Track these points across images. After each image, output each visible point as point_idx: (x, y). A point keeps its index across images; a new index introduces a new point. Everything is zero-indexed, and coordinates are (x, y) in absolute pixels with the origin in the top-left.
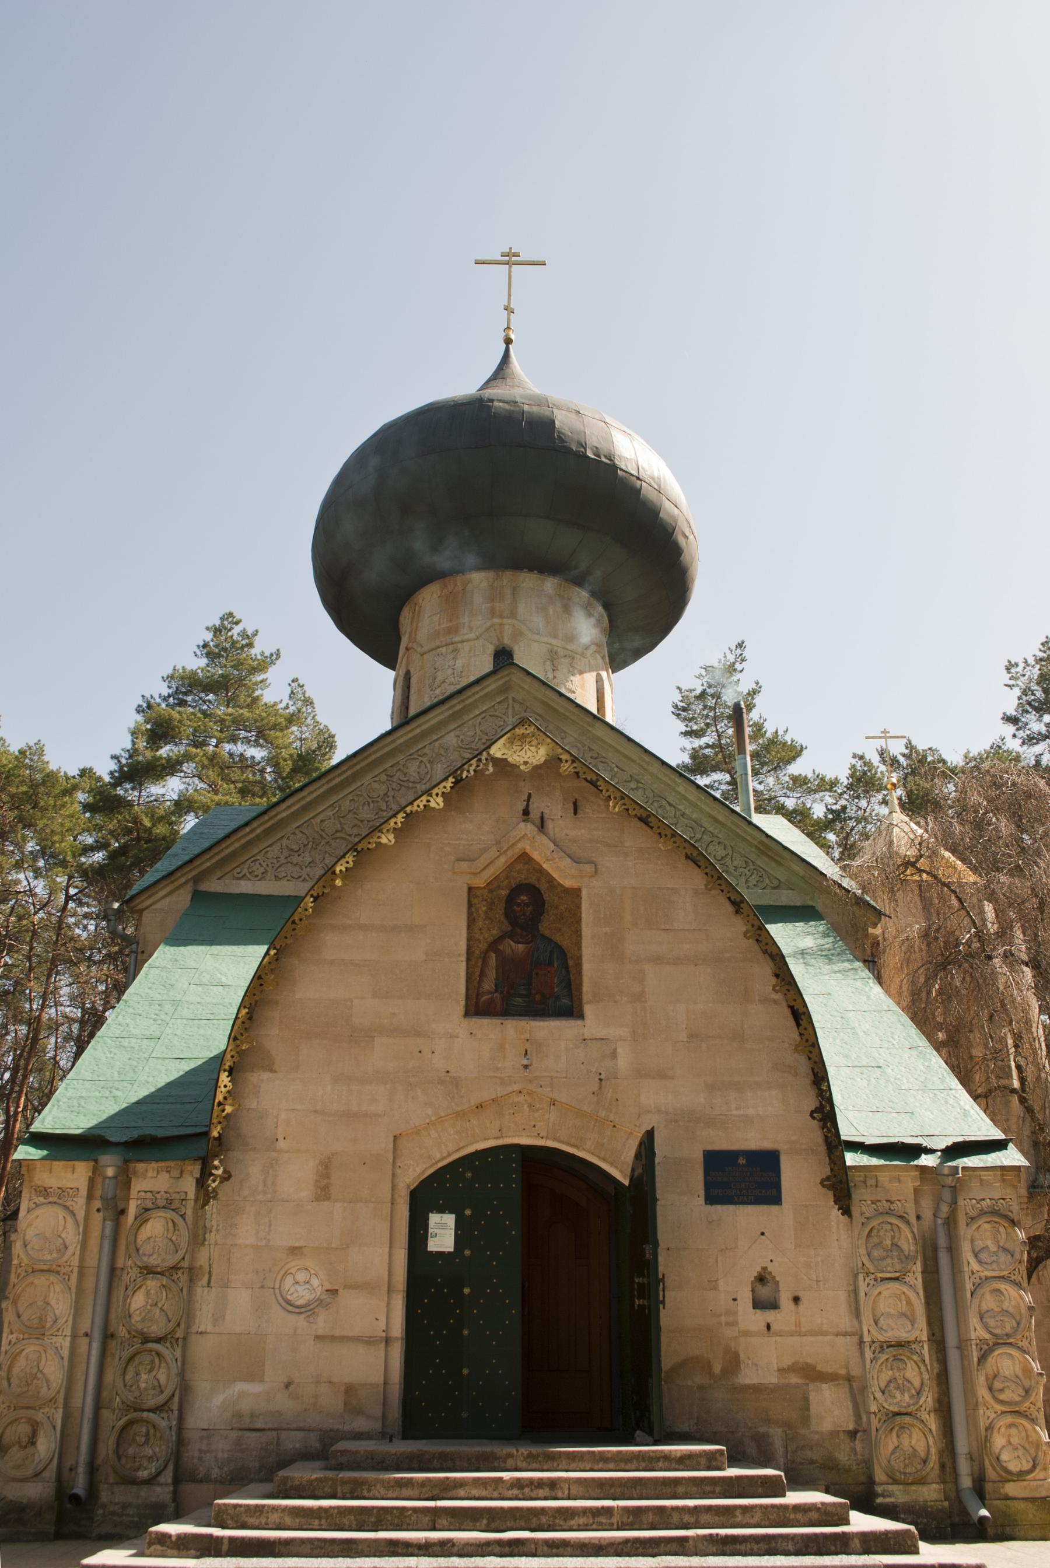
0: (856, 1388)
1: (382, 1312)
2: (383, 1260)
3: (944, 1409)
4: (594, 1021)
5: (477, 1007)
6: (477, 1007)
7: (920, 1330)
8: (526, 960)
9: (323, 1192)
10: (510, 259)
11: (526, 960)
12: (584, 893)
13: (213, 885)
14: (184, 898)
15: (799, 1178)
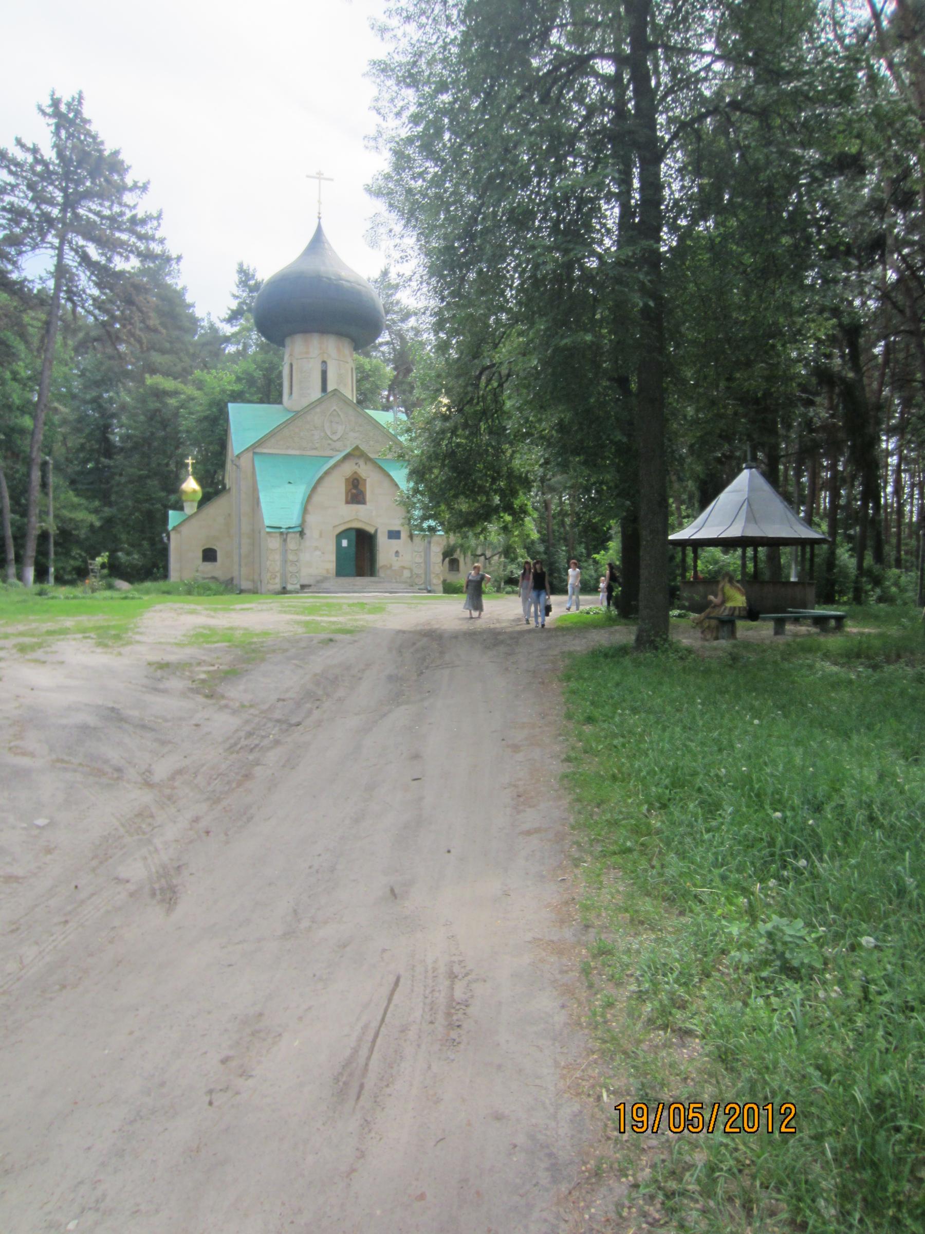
0: (411, 570)
1: (333, 558)
2: (331, 548)
3: (426, 574)
4: (369, 506)
5: (347, 502)
6: (347, 502)
7: (421, 560)
8: (356, 493)
9: (321, 536)
10: (319, 176)
11: (356, 493)
12: (368, 481)
13: (257, 450)
14: (250, 454)
15: (404, 535)
